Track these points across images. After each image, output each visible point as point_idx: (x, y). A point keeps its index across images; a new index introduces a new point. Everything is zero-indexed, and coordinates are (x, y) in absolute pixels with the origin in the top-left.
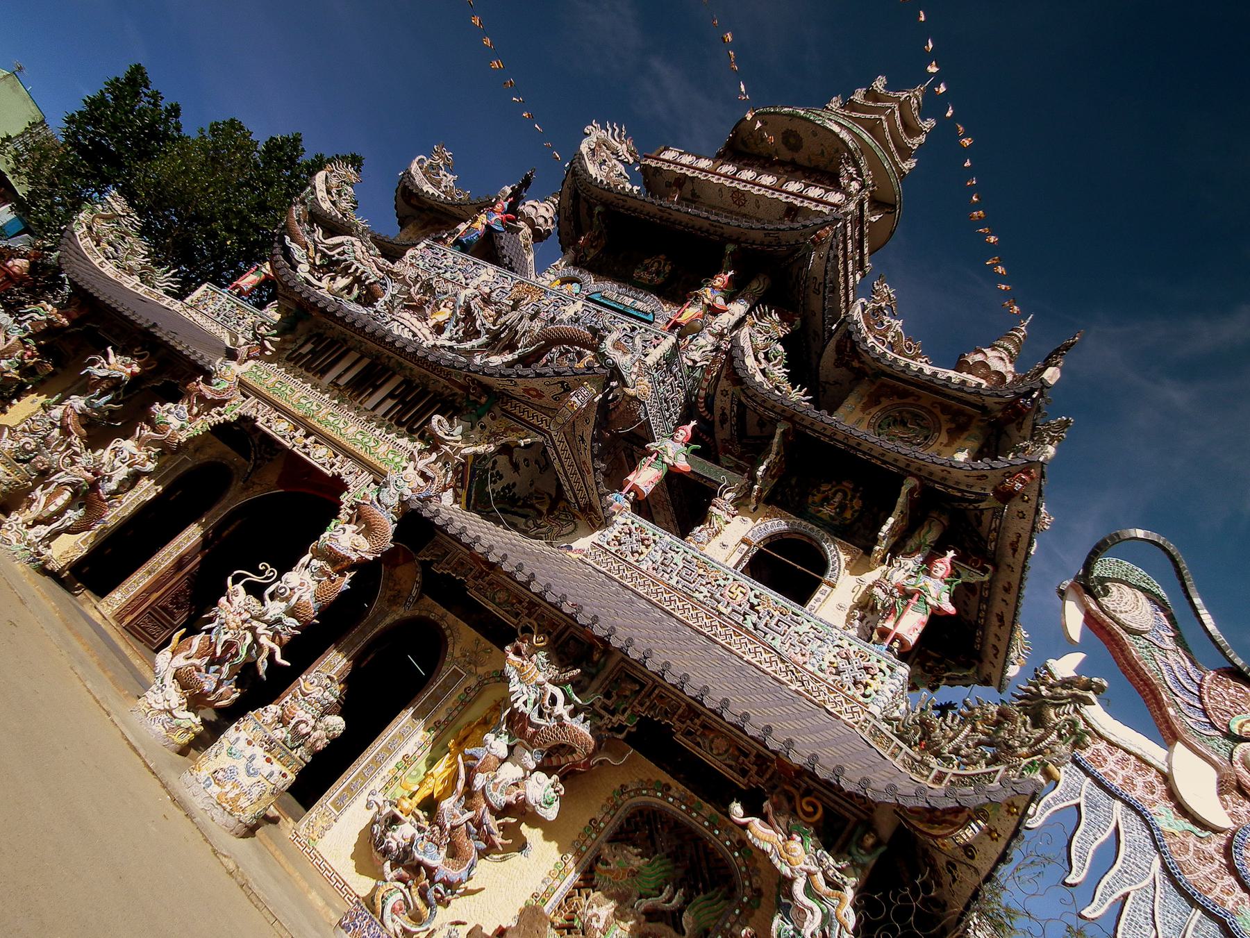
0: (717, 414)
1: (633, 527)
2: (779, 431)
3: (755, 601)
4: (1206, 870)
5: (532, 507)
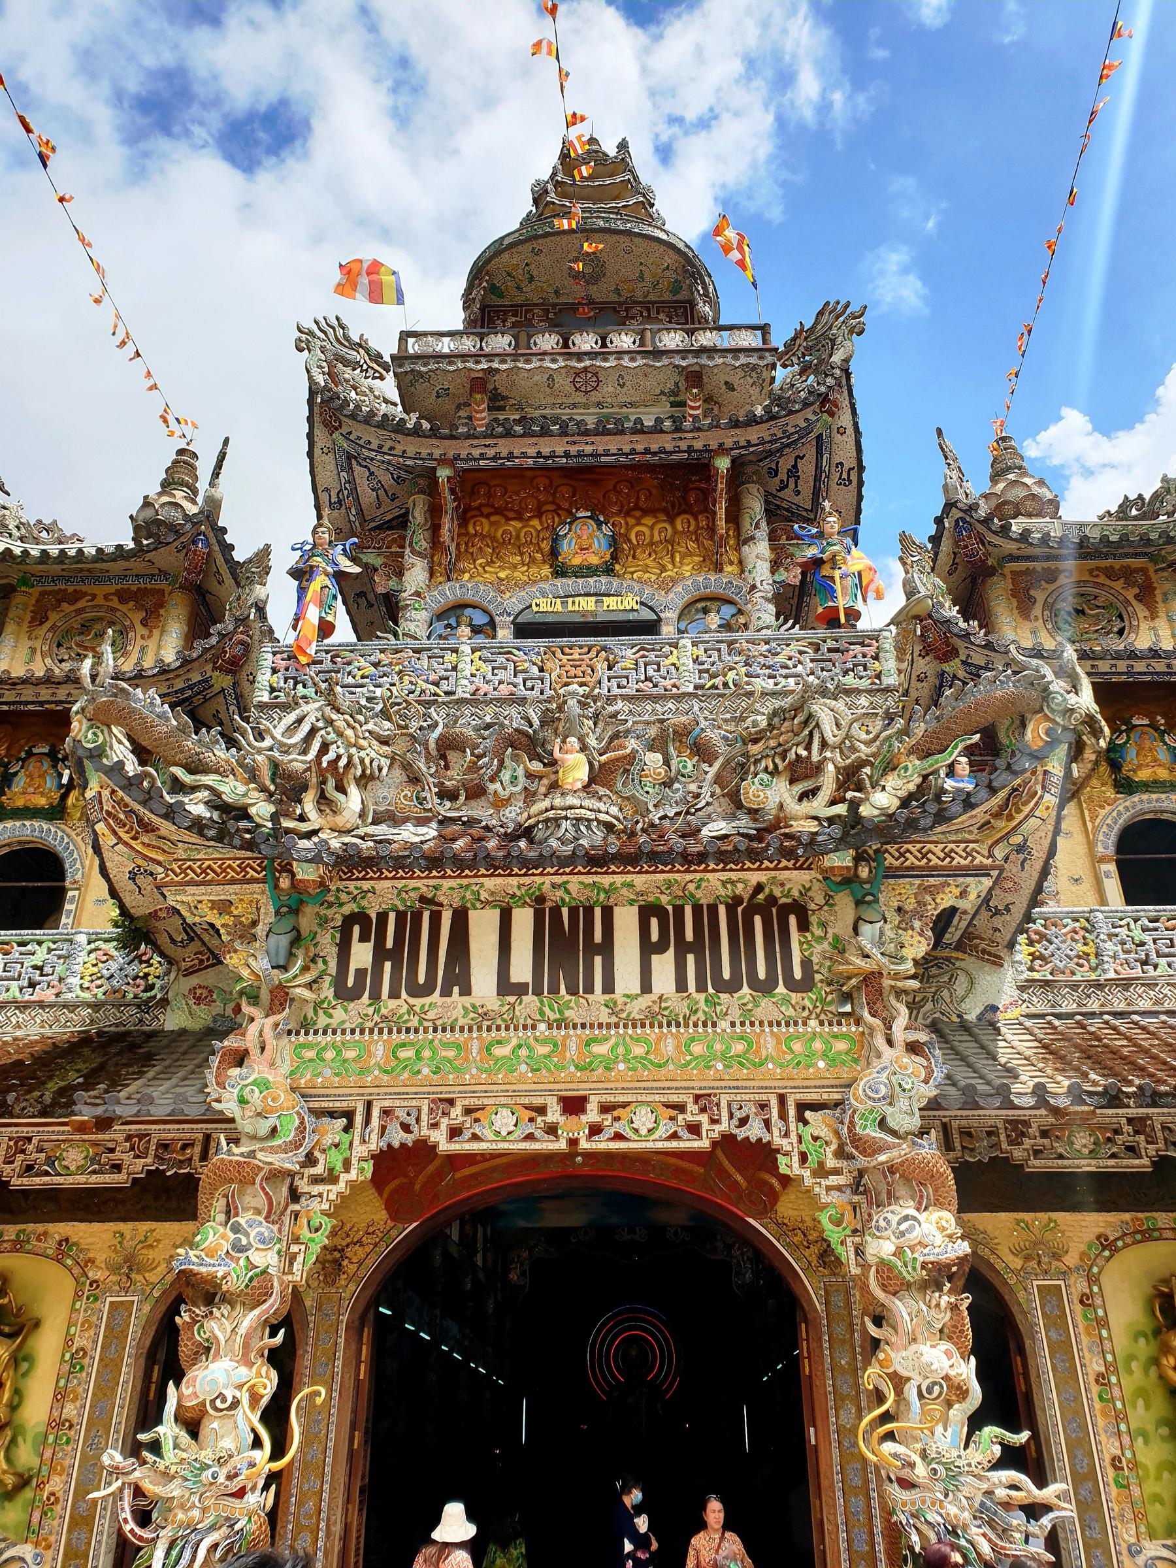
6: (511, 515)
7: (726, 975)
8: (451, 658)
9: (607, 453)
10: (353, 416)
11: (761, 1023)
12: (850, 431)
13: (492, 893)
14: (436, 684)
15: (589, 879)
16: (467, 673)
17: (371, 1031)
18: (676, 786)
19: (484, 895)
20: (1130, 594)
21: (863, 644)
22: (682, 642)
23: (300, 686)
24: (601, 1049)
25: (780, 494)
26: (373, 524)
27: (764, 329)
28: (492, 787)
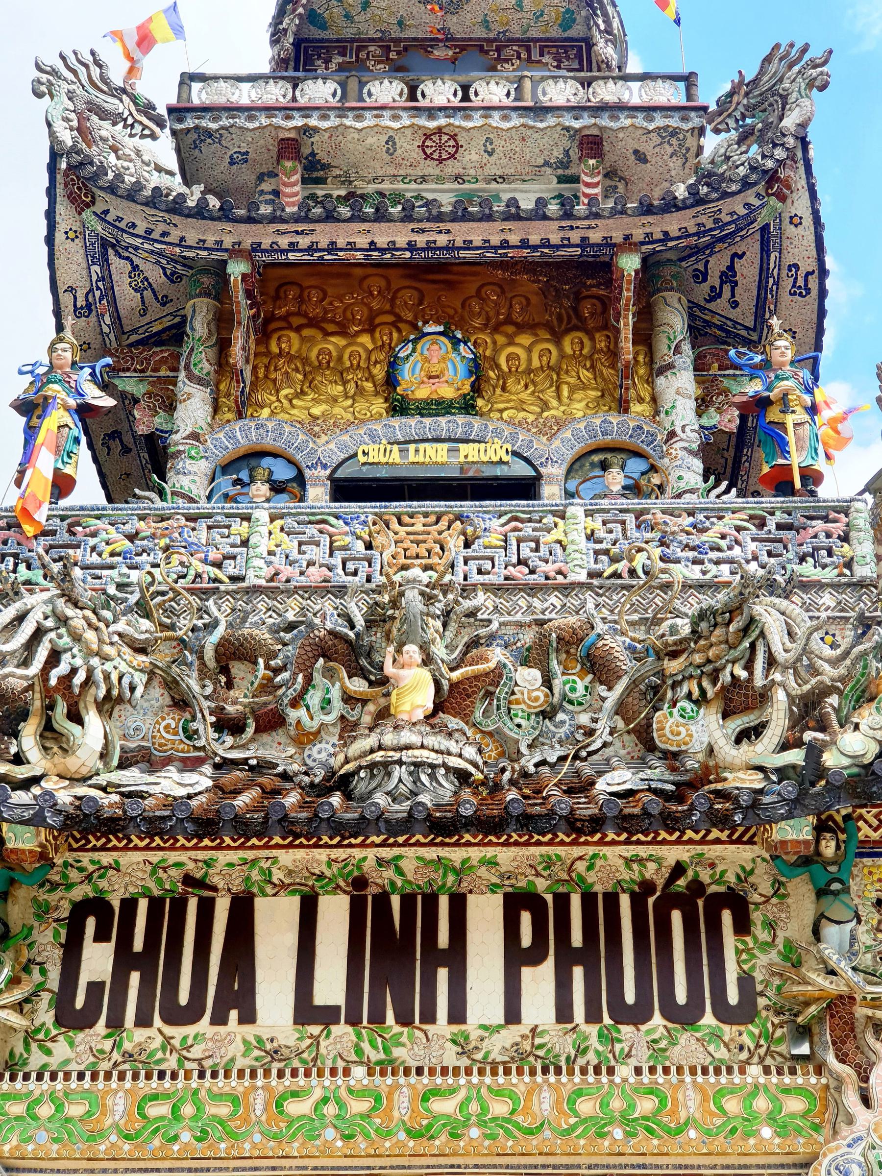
6: (331, 328)
7: (630, 997)
8: (240, 528)
9: (468, 245)
10: (112, 189)
11: (680, 1070)
12: (808, 221)
13: (290, 873)
14: (218, 565)
15: (431, 853)
16: (263, 550)
17: (108, 1076)
18: (561, 716)
19: (277, 876)
21: (826, 519)
22: (571, 510)
23: (22, 567)
24: (445, 1106)
25: (712, 306)
26: (134, 338)
27: (689, 80)
28: (293, 715)
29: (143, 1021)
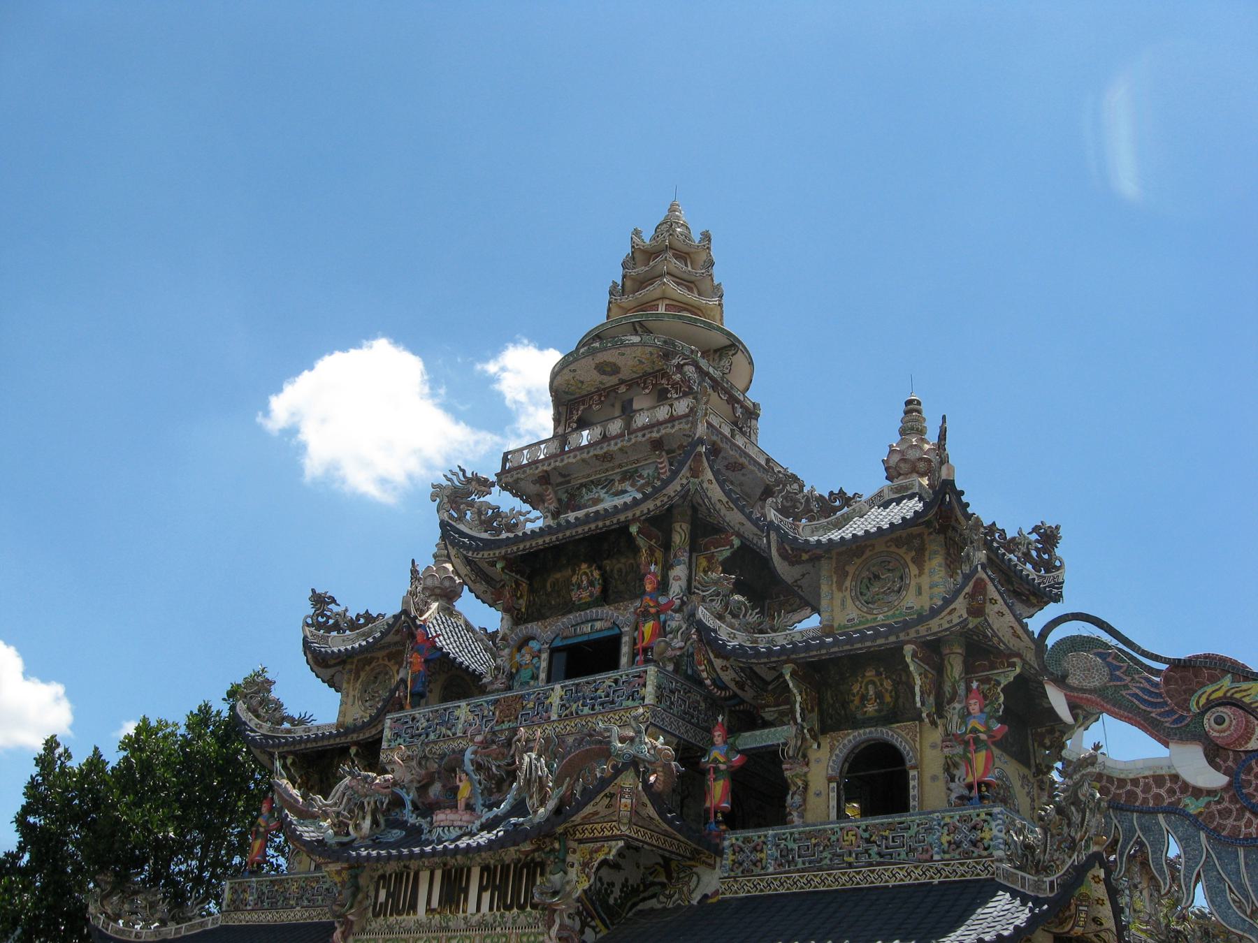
0: (732, 686)
1: (740, 843)
2: (787, 677)
3: (866, 835)
4: (1230, 822)
5: (653, 884)
20: (908, 560)
29: (391, 915)
